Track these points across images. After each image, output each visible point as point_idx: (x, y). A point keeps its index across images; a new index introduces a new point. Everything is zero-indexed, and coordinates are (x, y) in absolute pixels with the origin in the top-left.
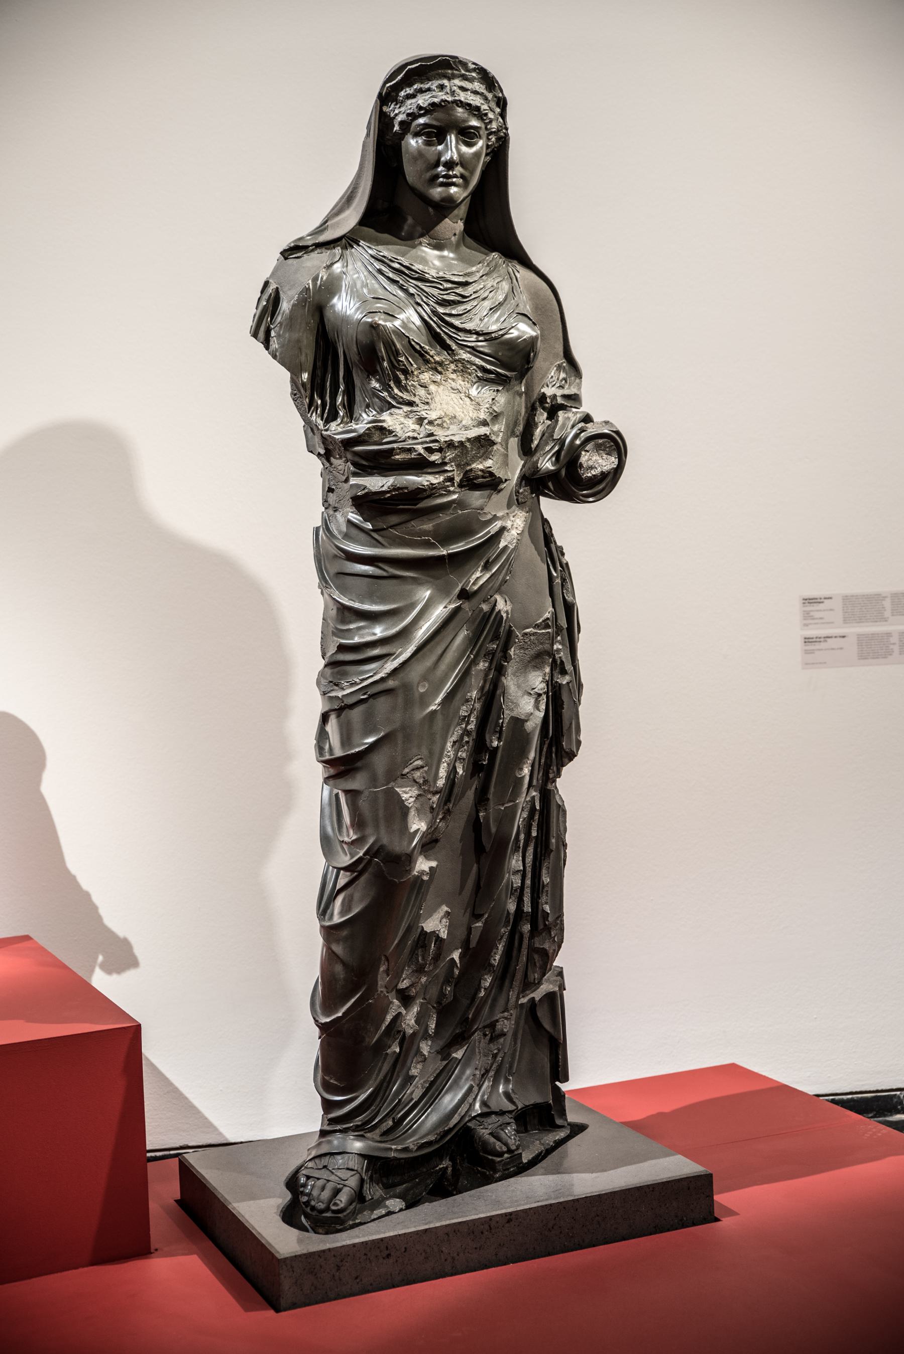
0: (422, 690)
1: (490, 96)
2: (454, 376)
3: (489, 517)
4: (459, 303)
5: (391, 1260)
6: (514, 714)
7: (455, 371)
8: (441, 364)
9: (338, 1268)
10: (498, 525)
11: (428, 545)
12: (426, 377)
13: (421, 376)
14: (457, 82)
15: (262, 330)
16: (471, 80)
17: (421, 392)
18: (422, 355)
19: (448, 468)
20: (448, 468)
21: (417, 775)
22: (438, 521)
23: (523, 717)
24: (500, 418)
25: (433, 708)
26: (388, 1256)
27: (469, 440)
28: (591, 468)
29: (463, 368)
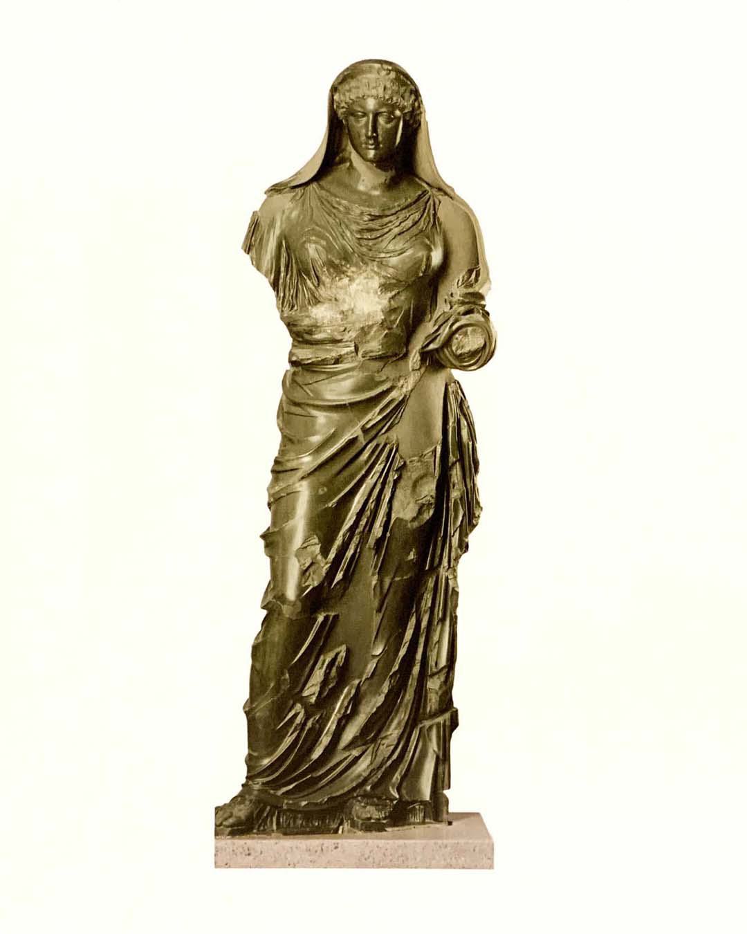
5: (251, 858)
6: (401, 516)
7: (365, 278)
15: (252, 243)
21: (313, 548)
26: (249, 854)
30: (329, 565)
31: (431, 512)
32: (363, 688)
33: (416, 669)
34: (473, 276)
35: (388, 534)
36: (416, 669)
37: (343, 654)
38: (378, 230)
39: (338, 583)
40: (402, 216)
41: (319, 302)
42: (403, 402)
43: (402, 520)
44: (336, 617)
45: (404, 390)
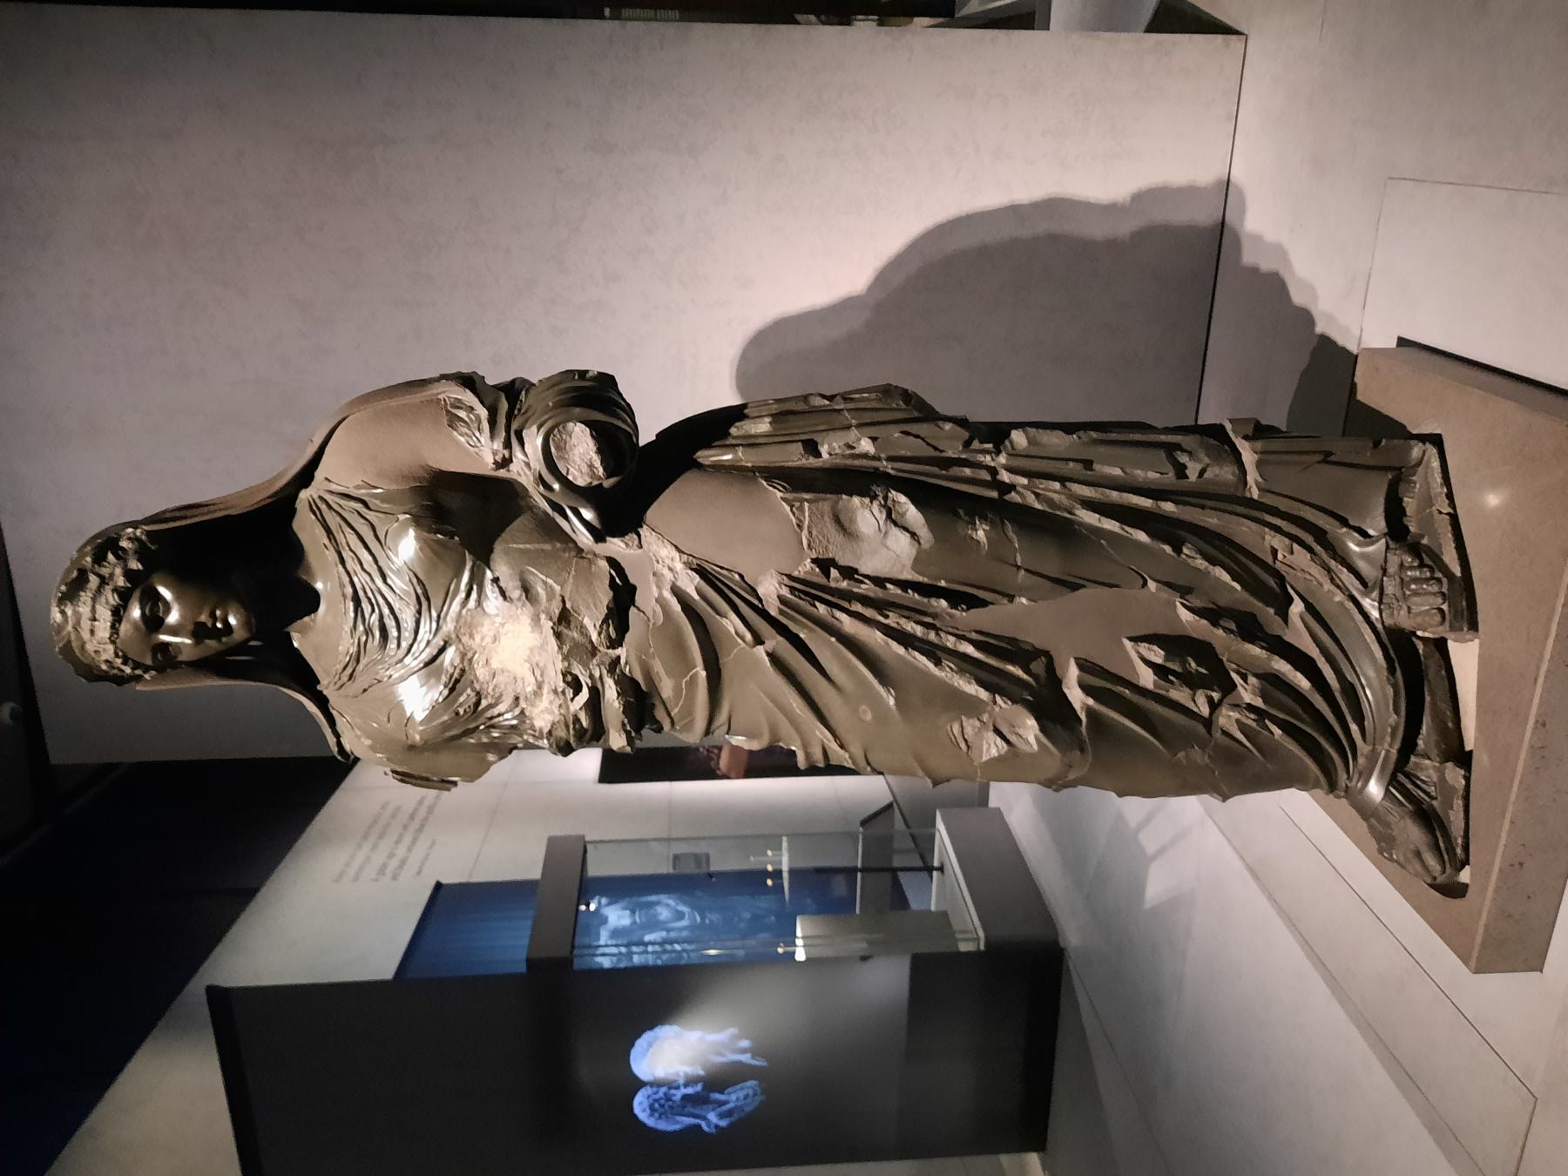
0: (869, 717)
1: (94, 581)
2: (478, 638)
3: (658, 609)
4: (381, 616)
6: (909, 563)
7: (471, 636)
8: (463, 656)
9: (1510, 916)
10: (667, 594)
11: (693, 681)
12: (481, 672)
13: (481, 678)
14: (86, 635)
16: (78, 616)
17: (500, 679)
18: (457, 681)
19: (597, 675)
20: (597, 675)
21: (969, 731)
22: (662, 673)
23: (914, 552)
24: (531, 578)
25: (892, 701)
27: (560, 648)
28: (591, 466)
29: (466, 627)
30: (998, 698)
31: (902, 498)
32: (1198, 603)
33: (1168, 507)
34: (462, 414)
35: (943, 583)
36: (1168, 507)
37: (1144, 648)
38: (381, 616)
39: (1028, 672)
40: (352, 564)
41: (522, 712)
42: (701, 571)
43: (916, 560)
44: (1083, 665)
45: (679, 566)
